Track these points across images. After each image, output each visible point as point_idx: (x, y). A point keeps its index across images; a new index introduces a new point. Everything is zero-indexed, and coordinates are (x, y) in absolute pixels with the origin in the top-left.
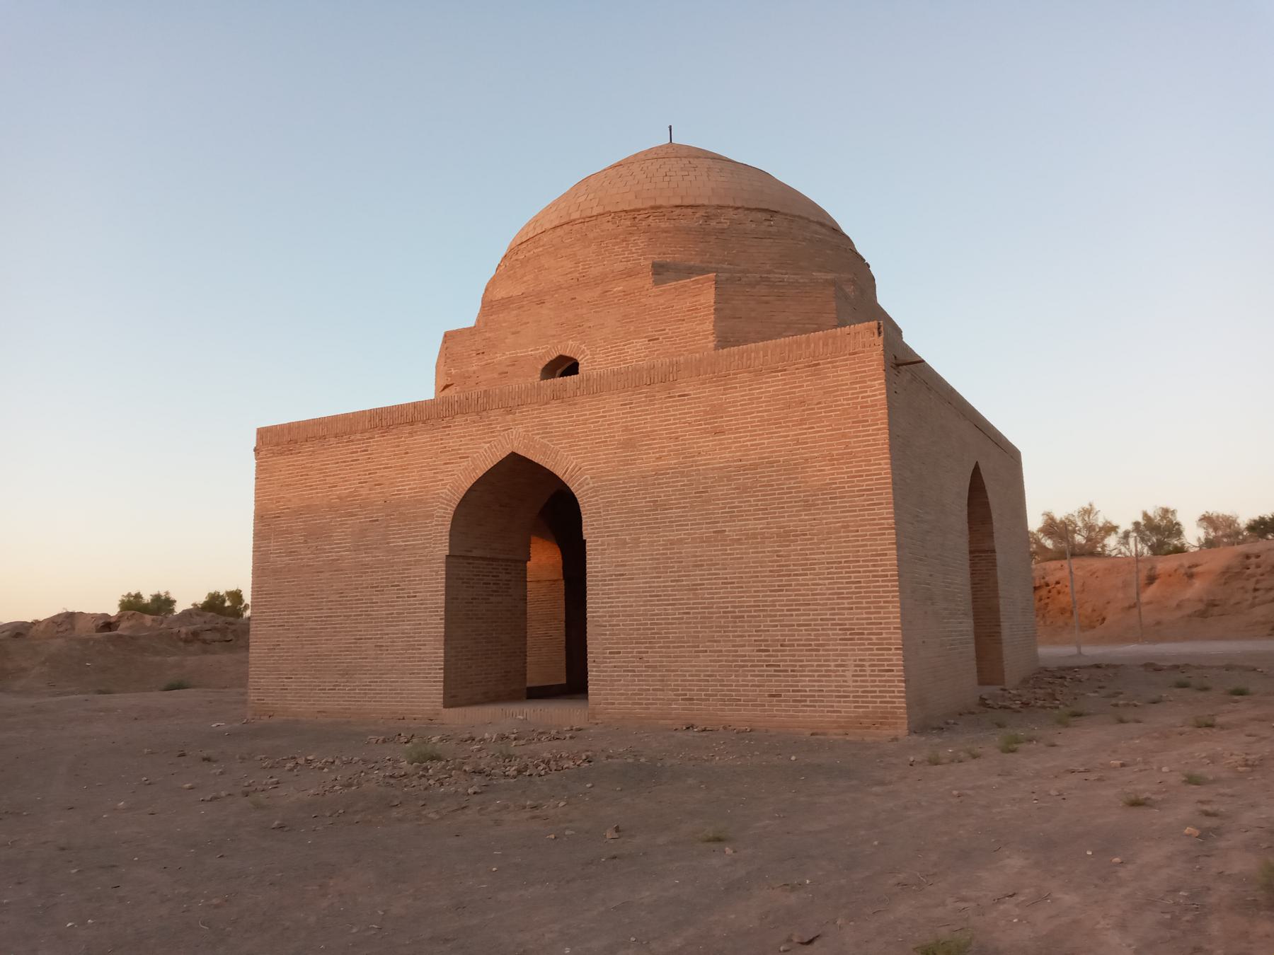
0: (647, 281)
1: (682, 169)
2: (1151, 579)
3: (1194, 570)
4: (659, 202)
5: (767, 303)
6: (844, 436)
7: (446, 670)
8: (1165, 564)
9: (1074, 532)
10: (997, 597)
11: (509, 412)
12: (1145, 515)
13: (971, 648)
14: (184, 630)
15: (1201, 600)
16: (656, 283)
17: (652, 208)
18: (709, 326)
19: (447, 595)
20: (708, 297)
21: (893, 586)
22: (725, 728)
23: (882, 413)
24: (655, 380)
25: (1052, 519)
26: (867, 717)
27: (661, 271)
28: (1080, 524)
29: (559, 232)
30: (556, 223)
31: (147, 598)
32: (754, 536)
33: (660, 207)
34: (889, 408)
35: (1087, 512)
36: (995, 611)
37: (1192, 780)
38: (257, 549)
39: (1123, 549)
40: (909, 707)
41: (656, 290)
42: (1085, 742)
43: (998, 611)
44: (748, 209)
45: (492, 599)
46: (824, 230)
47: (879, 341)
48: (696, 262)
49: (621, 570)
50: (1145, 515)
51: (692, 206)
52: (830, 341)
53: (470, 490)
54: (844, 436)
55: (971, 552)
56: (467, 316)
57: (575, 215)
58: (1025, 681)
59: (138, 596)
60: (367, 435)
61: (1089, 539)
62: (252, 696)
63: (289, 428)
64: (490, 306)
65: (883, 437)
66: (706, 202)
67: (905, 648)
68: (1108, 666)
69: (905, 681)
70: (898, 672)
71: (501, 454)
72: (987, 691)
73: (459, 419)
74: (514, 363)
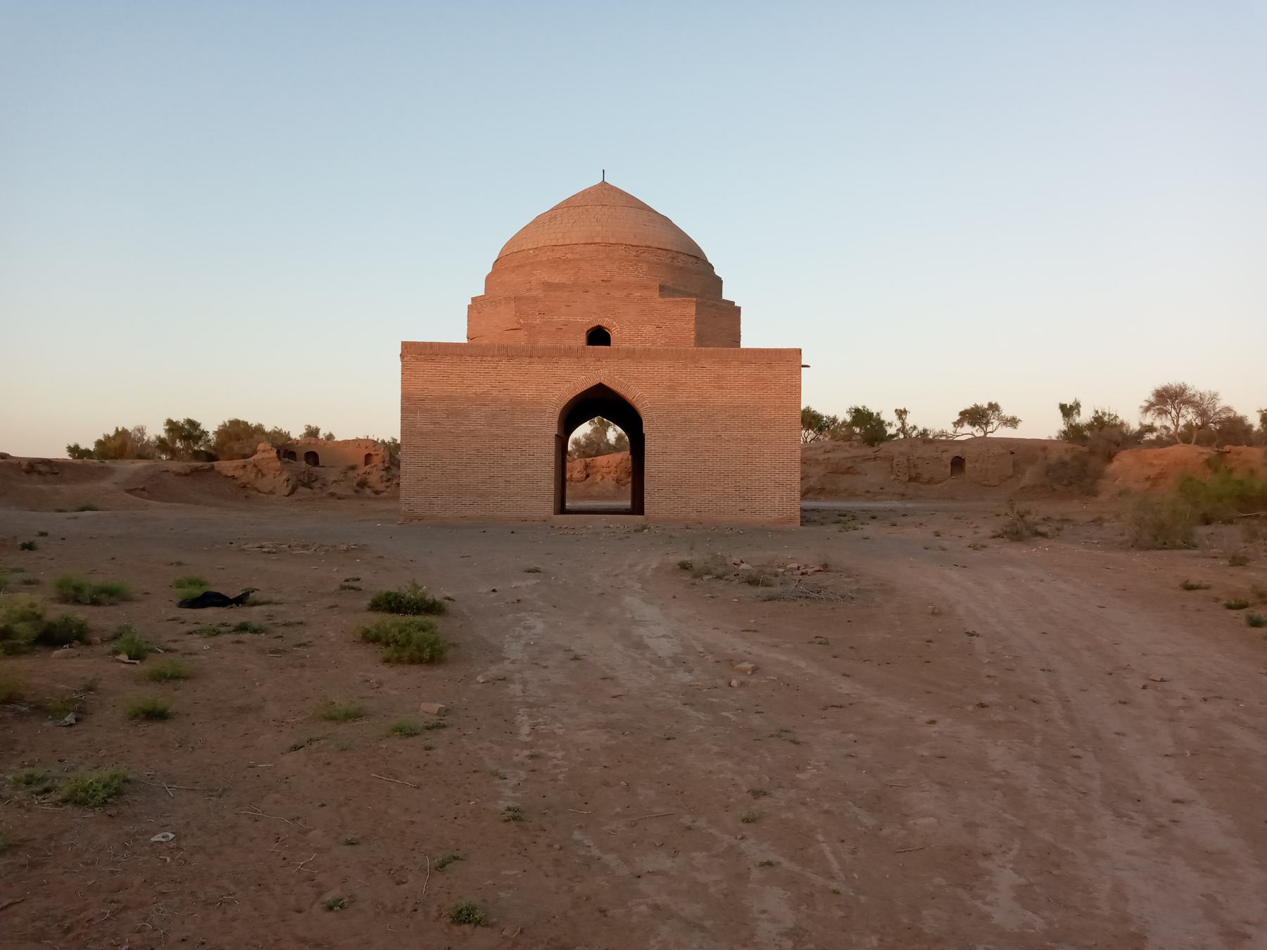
0: (657, 295)
4: (649, 244)
18: (692, 326)
20: (692, 310)
57: (598, 240)
63: (431, 345)
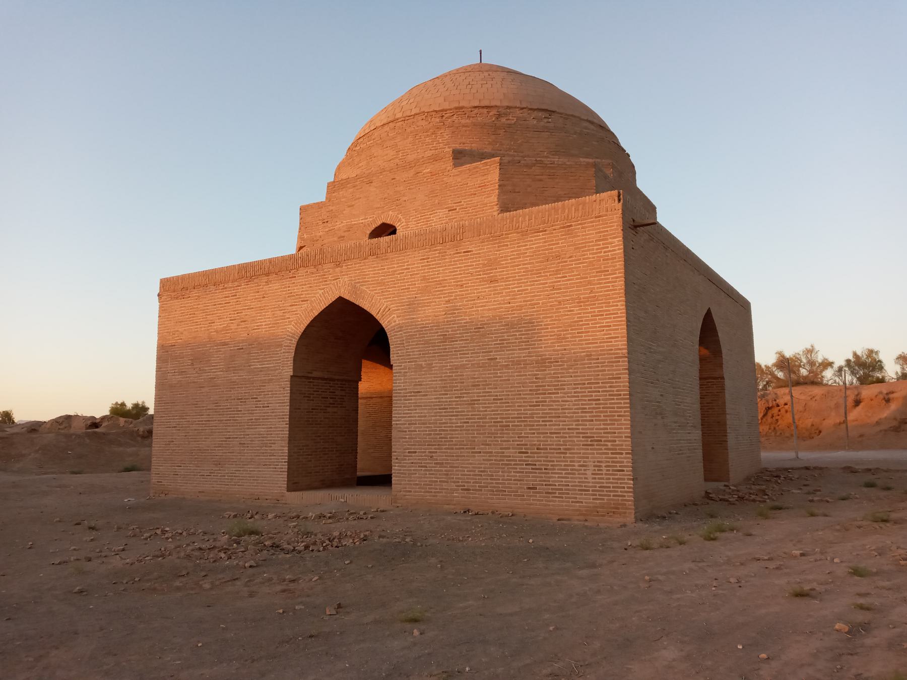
0: (449, 164)
1: (482, 80)
2: (857, 403)
3: (891, 396)
4: (461, 105)
5: (541, 180)
6: (590, 283)
7: (289, 463)
8: (868, 392)
9: (800, 366)
10: (724, 413)
11: (338, 266)
12: (855, 354)
13: (699, 453)
14: (141, 429)
15: (895, 419)
16: (456, 165)
17: (456, 108)
18: (494, 198)
19: (290, 406)
20: (494, 175)
21: (625, 403)
22: (493, 513)
23: (620, 265)
24: (449, 239)
25: (783, 356)
26: (603, 507)
27: (460, 157)
28: (804, 360)
29: (386, 128)
30: (385, 121)
31: (129, 405)
32: (518, 362)
33: (462, 108)
34: (625, 261)
35: (810, 351)
36: (722, 424)
37: (857, 572)
38: (159, 369)
39: (837, 380)
40: (637, 500)
41: (455, 171)
42: (777, 534)
43: (725, 424)
44: (531, 109)
45: (329, 410)
46: (592, 127)
47: (619, 206)
48: (489, 149)
49: (418, 388)
50: (855, 354)
51: (487, 107)
52: (580, 207)
53: (309, 326)
54: (590, 283)
55: (700, 379)
56: (320, 196)
57: (399, 115)
58: (748, 479)
59: (123, 404)
60: (236, 284)
61: (810, 372)
62: (154, 480)
64: (333, 188)
65: (620, 284)
66: (498, 104)
67: (633, 453)
68: (815, 468)
69: (633, 480)
70: (628, 471)
71: (331, 299)
72: (712, 486)
73: (302, 271)
74: (349, 229)
